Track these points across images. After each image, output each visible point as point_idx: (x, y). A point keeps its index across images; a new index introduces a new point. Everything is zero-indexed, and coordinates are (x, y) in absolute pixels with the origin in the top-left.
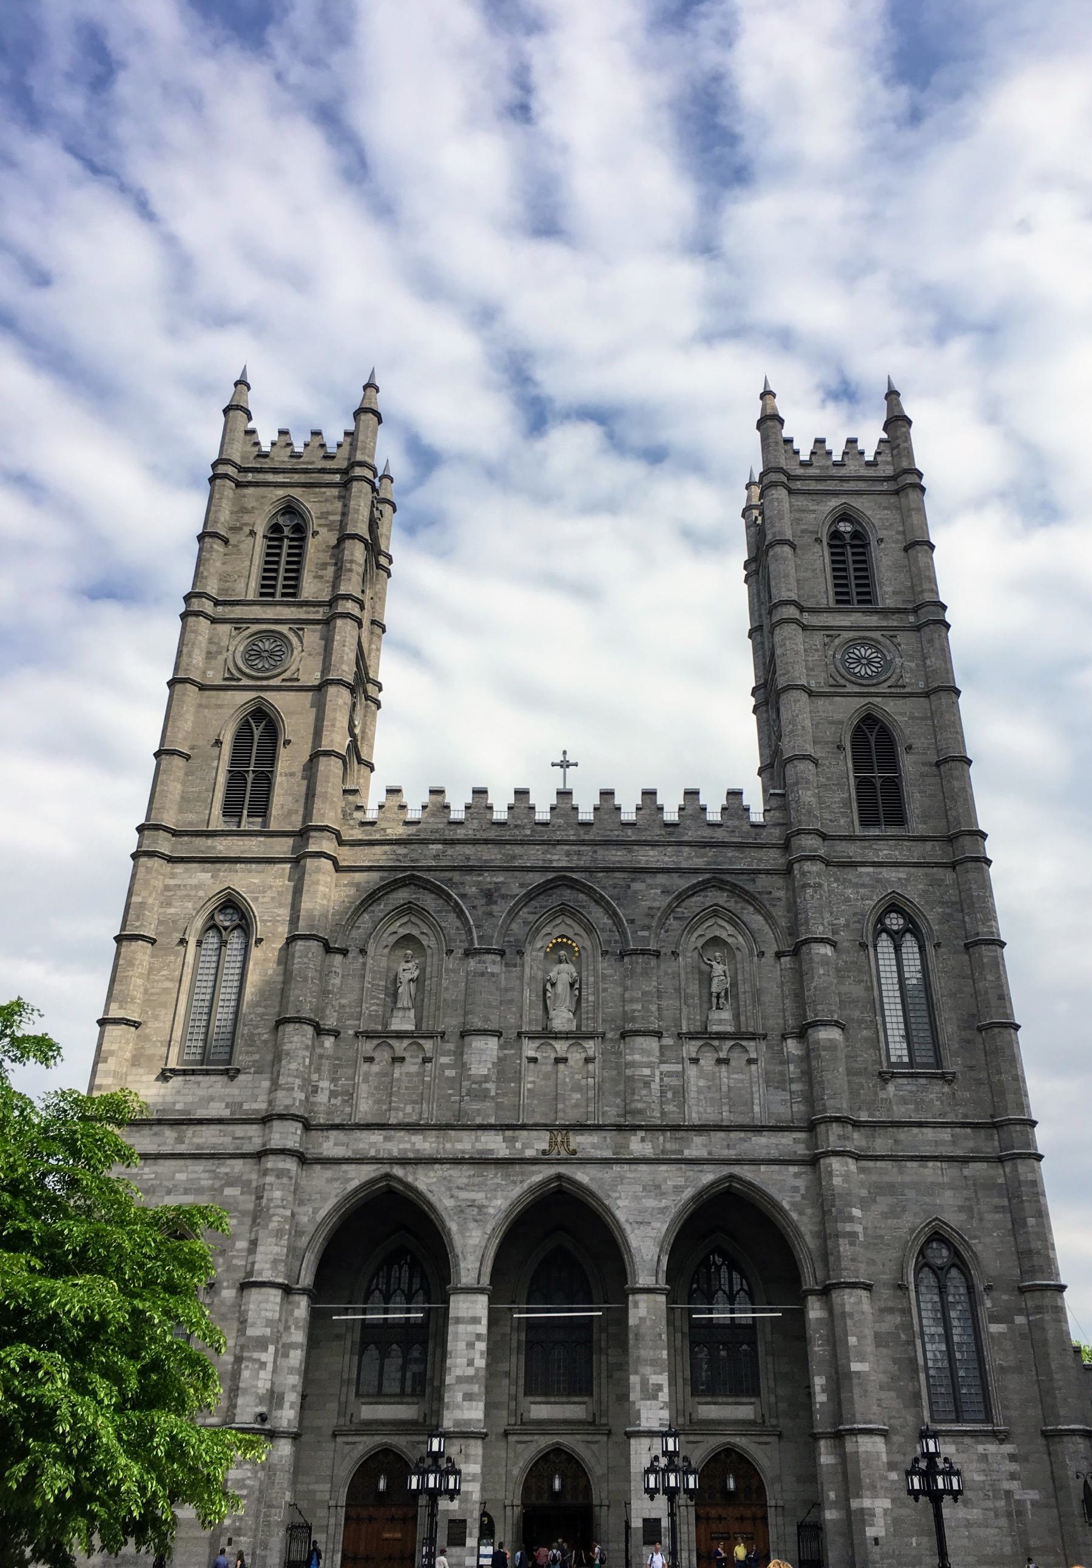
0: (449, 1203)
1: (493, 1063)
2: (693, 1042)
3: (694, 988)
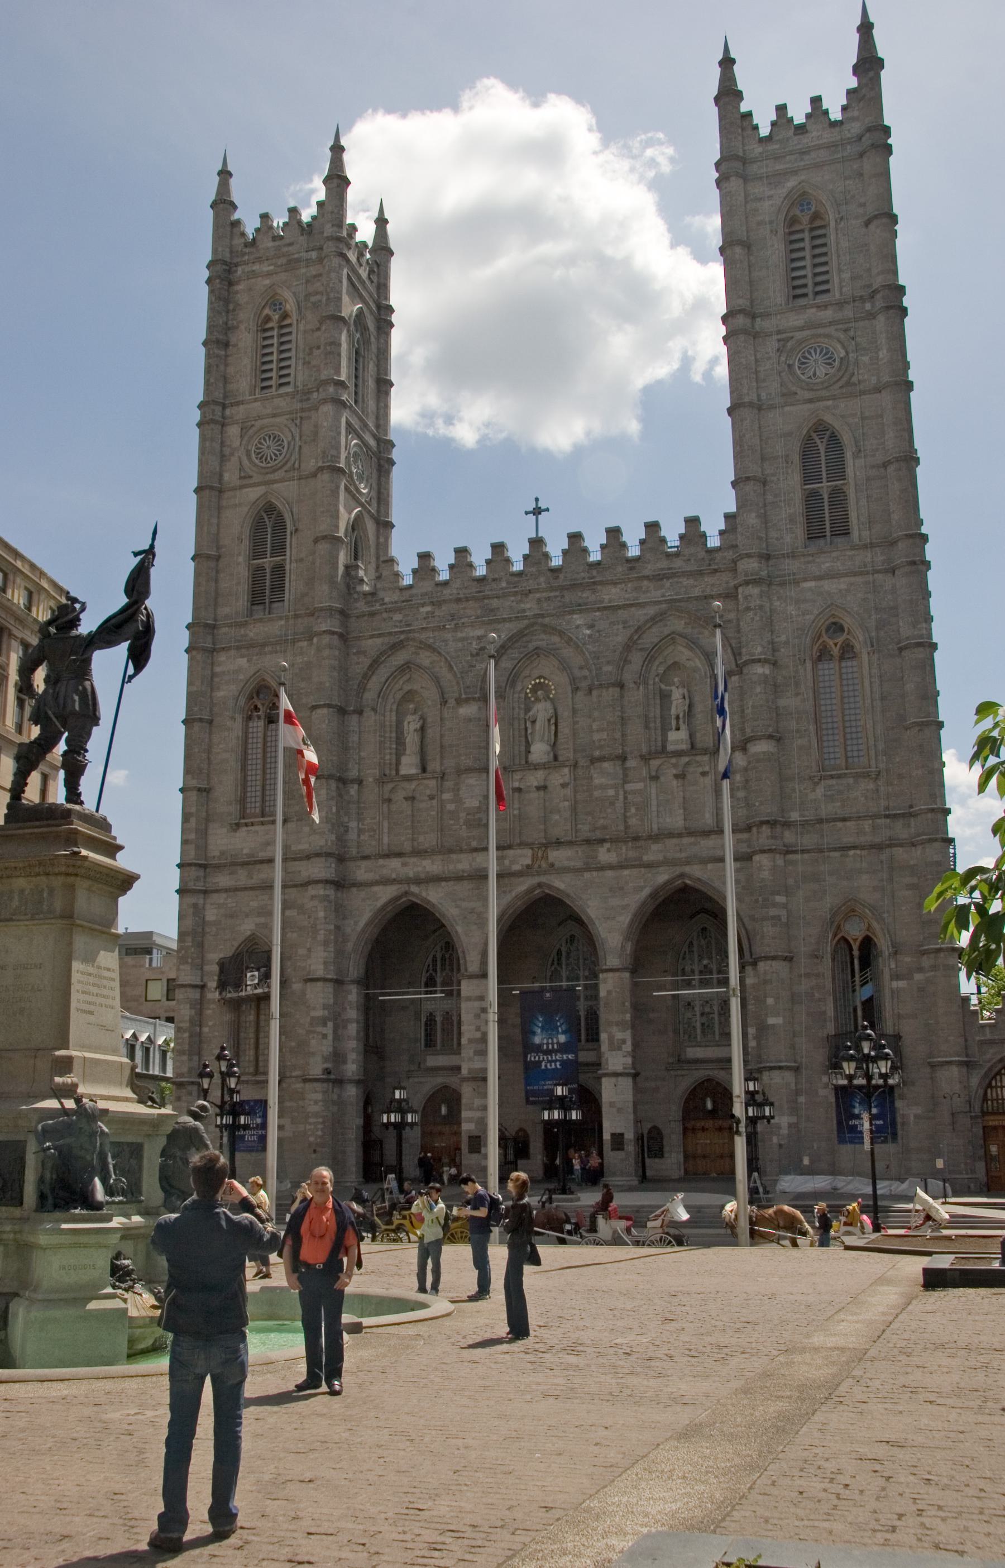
3: (656, 711)
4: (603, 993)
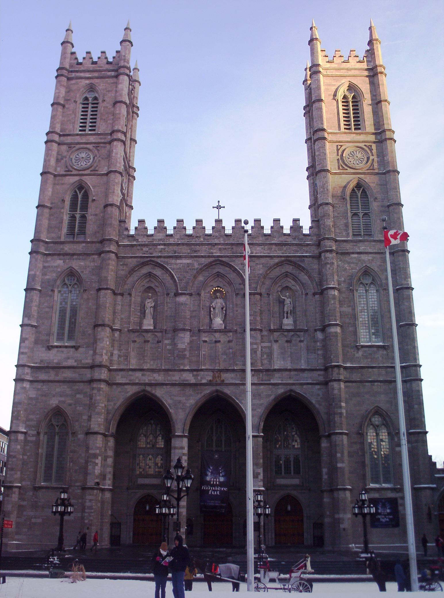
0: (170, 402)
1: (188, 343)
2: (275, 333)
3: (276, 309)
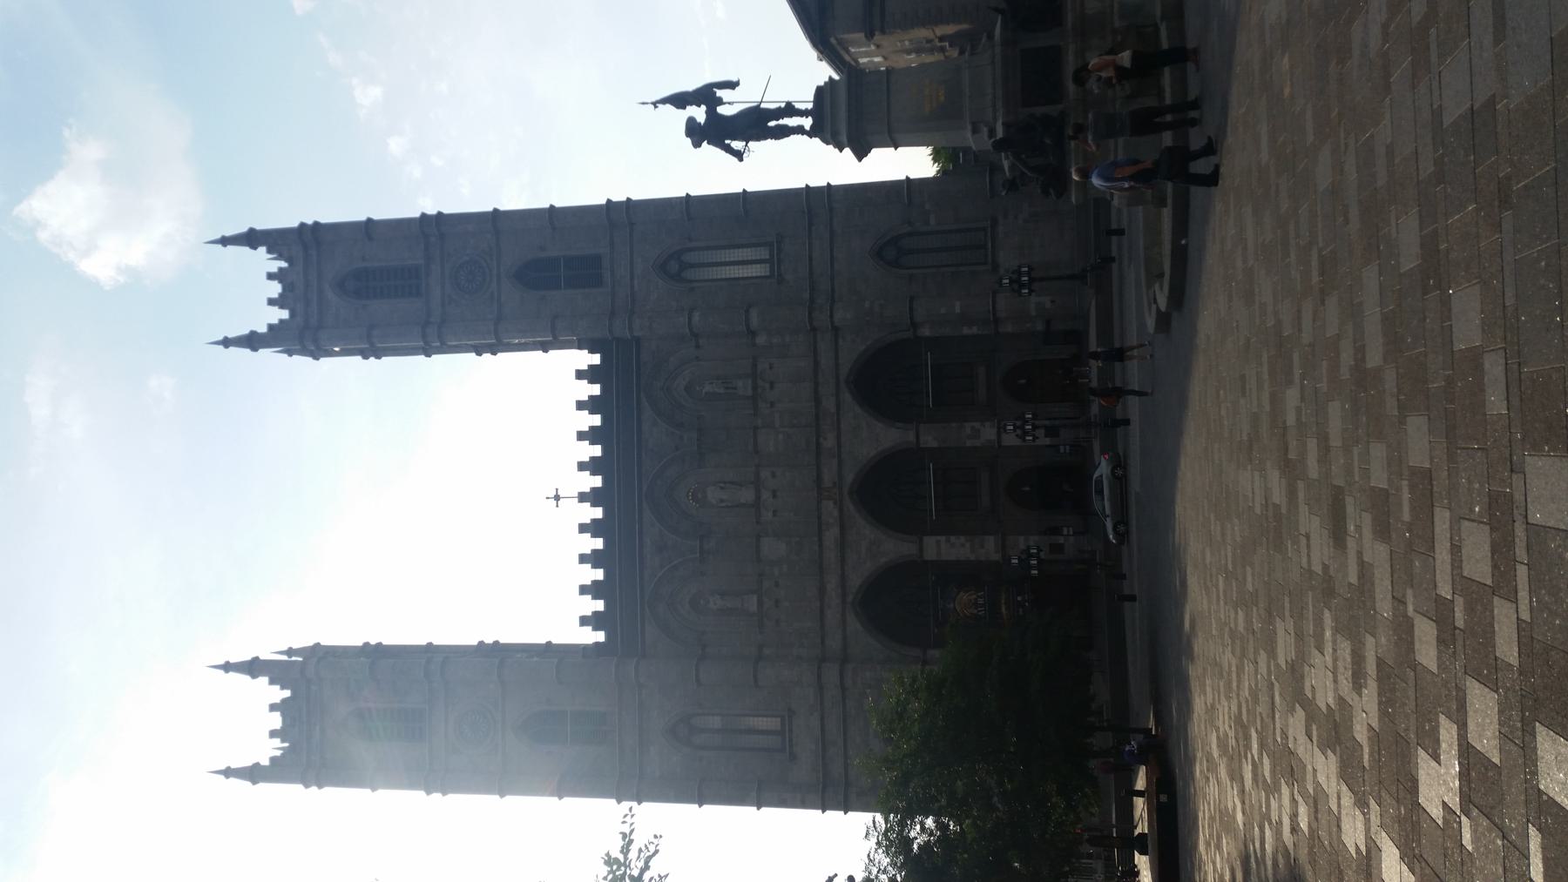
4: (935, 444)
